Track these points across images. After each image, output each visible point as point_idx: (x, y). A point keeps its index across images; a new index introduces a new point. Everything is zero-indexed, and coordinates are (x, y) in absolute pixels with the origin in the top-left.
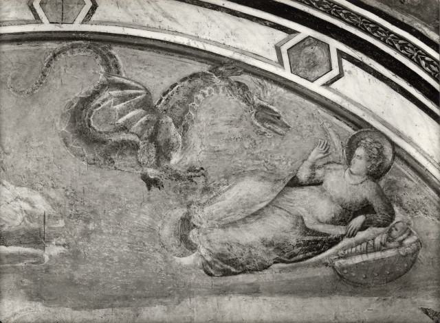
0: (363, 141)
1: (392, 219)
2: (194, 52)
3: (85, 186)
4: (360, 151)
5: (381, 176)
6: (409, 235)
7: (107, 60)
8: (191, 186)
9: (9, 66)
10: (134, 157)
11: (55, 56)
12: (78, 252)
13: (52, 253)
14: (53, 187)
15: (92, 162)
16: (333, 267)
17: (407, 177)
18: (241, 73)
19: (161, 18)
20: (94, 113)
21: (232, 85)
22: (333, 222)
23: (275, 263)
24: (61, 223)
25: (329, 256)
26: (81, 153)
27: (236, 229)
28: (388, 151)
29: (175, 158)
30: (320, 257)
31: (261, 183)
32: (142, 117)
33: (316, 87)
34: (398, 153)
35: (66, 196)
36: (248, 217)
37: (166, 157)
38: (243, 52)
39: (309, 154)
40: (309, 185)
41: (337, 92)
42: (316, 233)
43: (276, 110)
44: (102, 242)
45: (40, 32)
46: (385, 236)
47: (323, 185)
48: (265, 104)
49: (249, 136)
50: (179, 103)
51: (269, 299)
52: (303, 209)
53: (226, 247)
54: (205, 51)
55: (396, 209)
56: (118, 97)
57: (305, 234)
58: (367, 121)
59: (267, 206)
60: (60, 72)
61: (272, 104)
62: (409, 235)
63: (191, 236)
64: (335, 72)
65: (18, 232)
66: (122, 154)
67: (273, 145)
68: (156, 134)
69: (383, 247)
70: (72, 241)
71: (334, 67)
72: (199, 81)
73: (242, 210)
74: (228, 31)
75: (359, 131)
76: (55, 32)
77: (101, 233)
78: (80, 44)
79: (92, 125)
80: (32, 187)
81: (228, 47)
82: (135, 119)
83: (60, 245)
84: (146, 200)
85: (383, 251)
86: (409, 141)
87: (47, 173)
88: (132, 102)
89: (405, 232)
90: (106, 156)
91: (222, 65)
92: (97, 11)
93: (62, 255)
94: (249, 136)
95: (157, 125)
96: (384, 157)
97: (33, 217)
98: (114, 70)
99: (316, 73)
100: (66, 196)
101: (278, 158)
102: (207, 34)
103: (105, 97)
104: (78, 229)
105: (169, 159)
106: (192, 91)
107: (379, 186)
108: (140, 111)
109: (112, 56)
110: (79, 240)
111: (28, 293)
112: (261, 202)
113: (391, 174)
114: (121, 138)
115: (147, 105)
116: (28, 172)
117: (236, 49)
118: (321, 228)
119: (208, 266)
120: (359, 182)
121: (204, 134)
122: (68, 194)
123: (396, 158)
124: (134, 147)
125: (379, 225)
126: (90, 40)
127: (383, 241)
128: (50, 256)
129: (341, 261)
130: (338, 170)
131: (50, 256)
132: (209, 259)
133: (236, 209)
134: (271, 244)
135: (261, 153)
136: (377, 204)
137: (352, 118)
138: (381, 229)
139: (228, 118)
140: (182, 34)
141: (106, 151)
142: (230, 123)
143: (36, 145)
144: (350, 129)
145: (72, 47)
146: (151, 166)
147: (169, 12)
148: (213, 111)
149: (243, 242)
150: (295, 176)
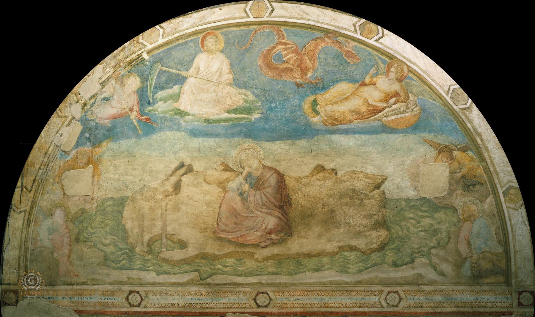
0: (394, 65)
1: (408, 99)
2: (317, 28)
3: (270, 88)
4: (393, 69)
5: (403, 80)
6: (416, 106)
7: (278, 33)
8: (317, 87)
9: (236, 37)
10: (291, 75)
11: (256, 32)
12: (267, 116)
13: (256, 117)
14: (256, 89)
15: (273, 77)
16: (382, 121)
17: (415, 80)
18: (338, 37)
19: (302, 14)
20: (273, 56)
21: (334, 42)
22: (381, 101)
23: (355, 119)
24: (260, 104)
25: (380, 116)
26: (268, 73)
27: (337, 105)
28: (405, 69)
29: (310, 75)
30: (375, 117)
31: (348, 85)
32: (294, 57)
33: (372, 42)
34: (410, 70)
35: (262, 92)
36: (343, 99)
37: (305, 74)
38: (339, 27)
39: (370, 71)
40: (370, 85)
41: (381, 44)
42: (373, 106)
43: (354, 52)
44: (277, 112)
45: (249, 22)
46: (405, 107)
47: (376, 85)
48: (349, 50)
49: (342, 64)
50: (311, 50)
51: (353, 135)
52: (367, 96)
53: (333, 113)
54: (322, 27)
55: (410, 95)
56: (284, 49)
57: (369, 107)
58: (396, 56)
59: (351, 95)
60: (258, 39)
61: (352, 50)
62: (416, 106)
63: (317, 108)
64: (381, 35)
65: (240, 108)
66: (286, 73)
67: (353, 68)
68: (301, 64)
69: (404, 112)
70: (264, 111)
71: (380, 33)
72: (319, 41)
73: (340, 97)
74: (332, 18)
75: (392, 60)
76: (256, 21)
77: (277, 108)
78: (267, 26)
79: (272, 61)
80: (246, 88)
81: (332, 26)
82: (291, 58)
83: (259, 113)
84: (297, 93)
85: (404, 113)
86: (415, 64)
87: (253, 82)
88: (290, 50)
89: (414, 105)
90: (279, 74)
91: (329, 33)
92: (274, 12)
93: (260, 118)
94: (342, 64)
95: (301, 60)
96: (404, 72)
97: (247, 101)
98: (282, 37)
99: (372, 36)
100: (262, 92)
101: (356, 73)
102: (323, 19)
103: (278, 49)
104: (267, 107)
105: (307, 75)
106: (317, 45)
107: (402, 85)
108: (294, 54)
109: (281, 31)
110: (267, 111)
111: (245, 135)
112: (348, 93)
113: (407, 79)
114: (286, 66)
115: (296, 52)
116: (245, 82)
117: (336, 26)
118: (376, 104)
119: (325, 121)
120: (393, 82)
121: (322, 63)
122: (262, 91)
123: (409, 72)
124: (291, 70)
125: (402, 102)
126: (271, 24)
127: (404, 109)
128: (255, 119)
129: (385, 118)
130: (383, 78)
131: (255, 119)
132: (325, 118)
133: (337, 96)
134: (353, 111)
135: (348, 71)
136: (401, 93)
137: (388, 55)
138: (403, 104)
139: (333, 56)
140: (311, 20)
141: (279, 72)
142: (334, 58)
143: (248, 70)
144: (388, 60)
145: (263, 28)
146: (299, 78)
147: (306, 11)
148: (326, 53)
149: (341, 111)
150: (364, 81)
